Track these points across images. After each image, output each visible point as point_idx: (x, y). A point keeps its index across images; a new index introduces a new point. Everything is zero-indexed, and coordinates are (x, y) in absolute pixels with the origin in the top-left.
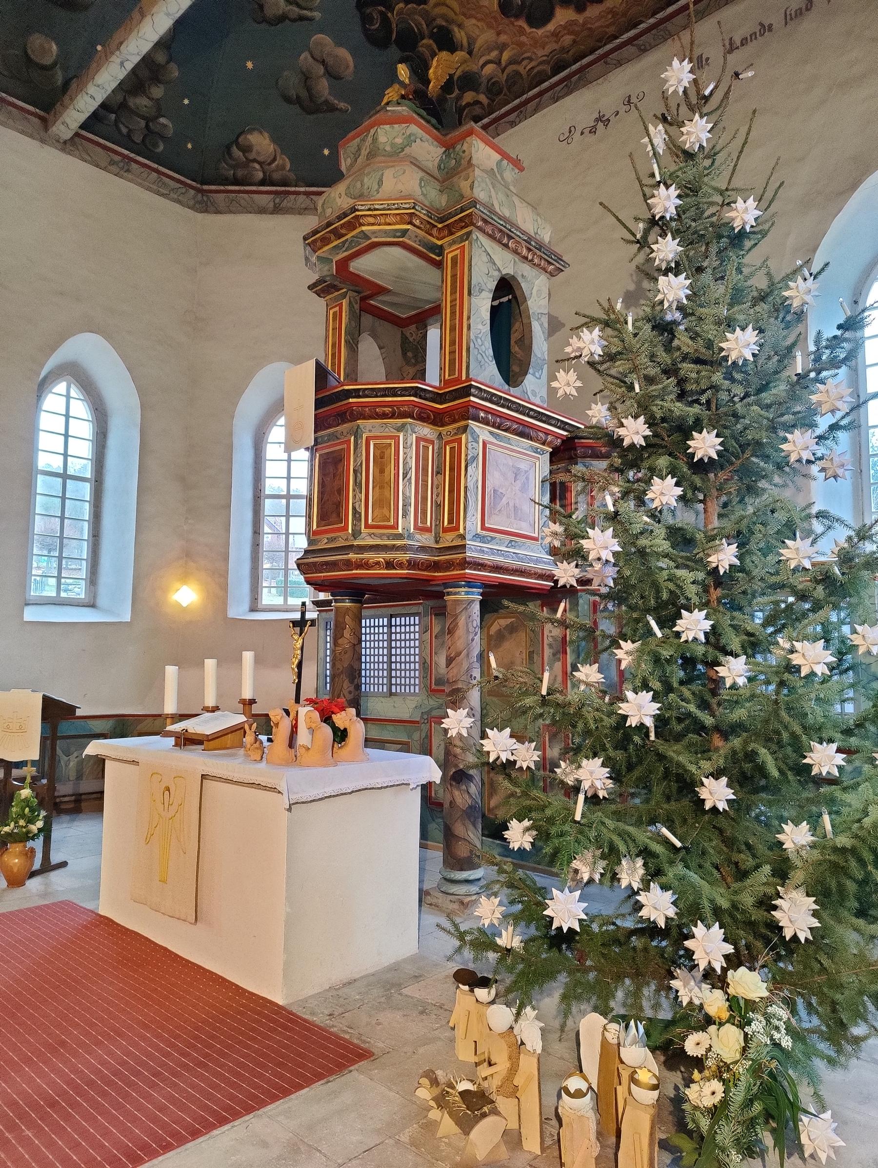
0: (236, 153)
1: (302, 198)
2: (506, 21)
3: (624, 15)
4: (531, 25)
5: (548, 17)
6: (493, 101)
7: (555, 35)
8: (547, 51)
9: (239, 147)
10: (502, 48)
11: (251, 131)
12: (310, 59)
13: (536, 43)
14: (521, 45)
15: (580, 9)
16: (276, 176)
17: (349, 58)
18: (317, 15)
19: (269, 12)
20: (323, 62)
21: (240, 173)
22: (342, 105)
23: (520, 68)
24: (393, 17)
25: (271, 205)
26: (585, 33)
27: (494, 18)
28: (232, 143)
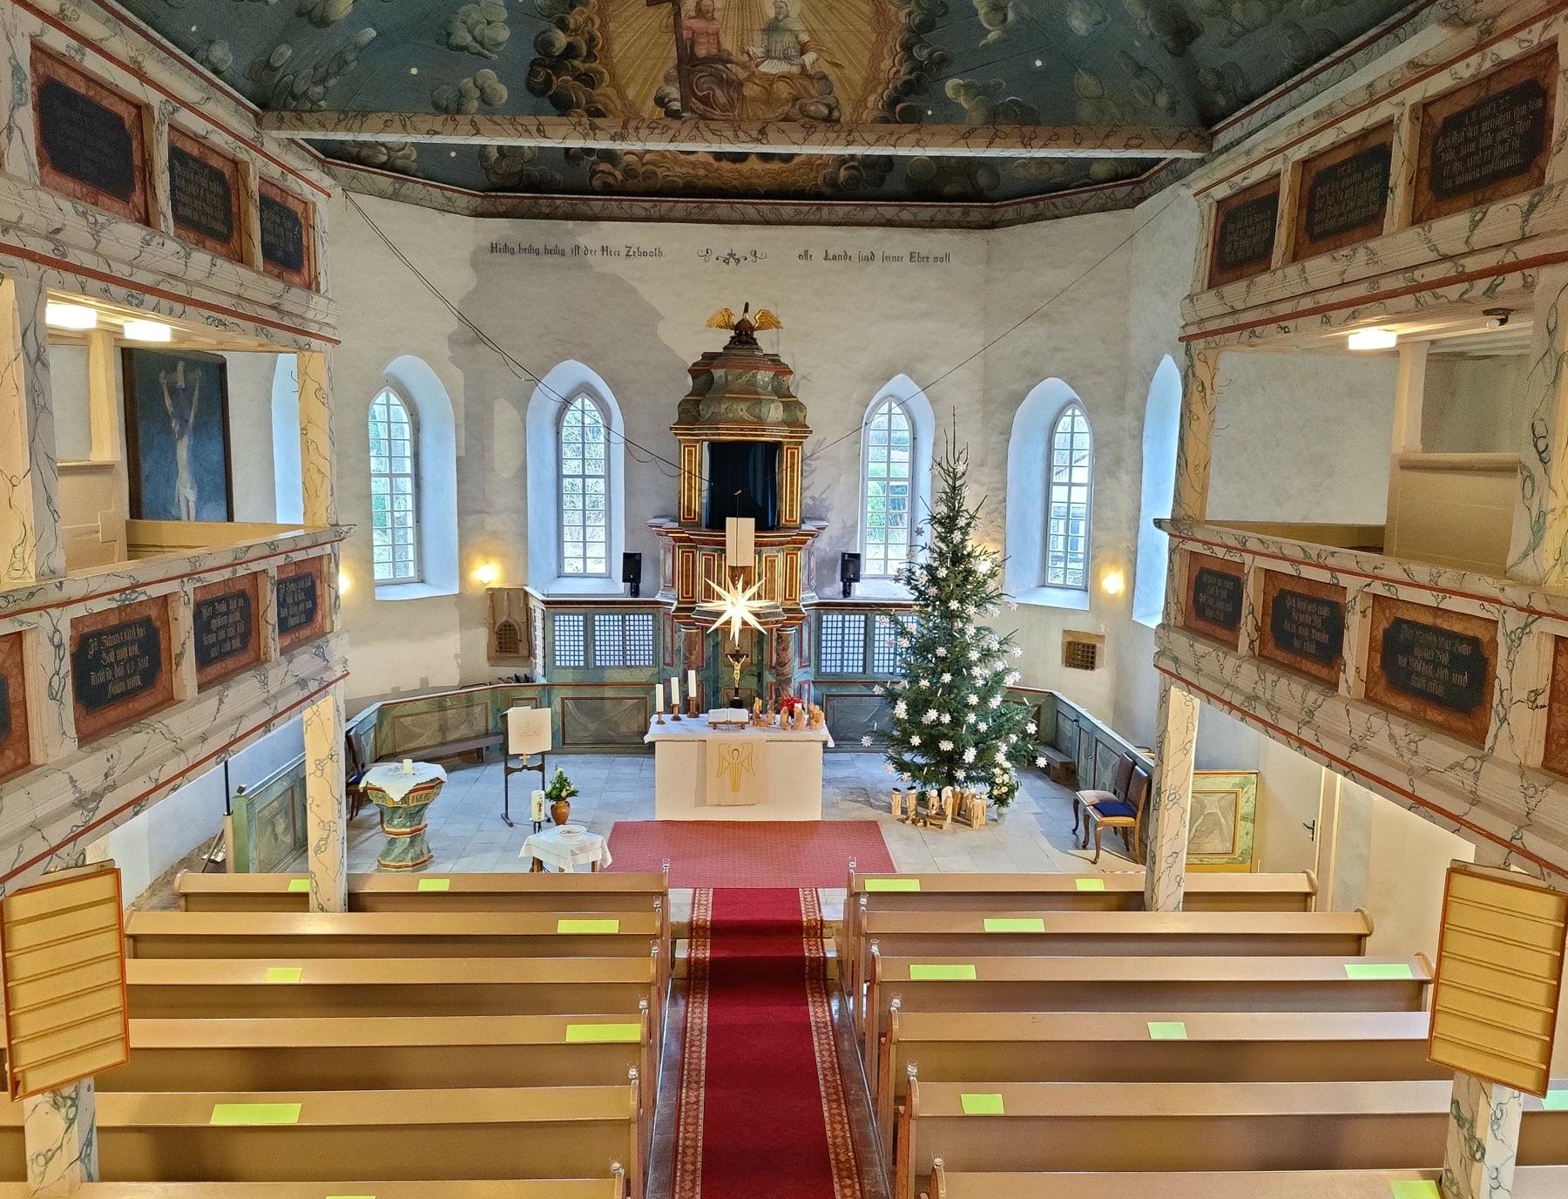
8: (684, 170)
12: (471, 84)
16: (400, 163)
17: (505, 94)
18: (495, 57)
19: (453, 40)
20: (481, 90)
23: (659, 171)
24: (556, 82)
25: (390, 190)
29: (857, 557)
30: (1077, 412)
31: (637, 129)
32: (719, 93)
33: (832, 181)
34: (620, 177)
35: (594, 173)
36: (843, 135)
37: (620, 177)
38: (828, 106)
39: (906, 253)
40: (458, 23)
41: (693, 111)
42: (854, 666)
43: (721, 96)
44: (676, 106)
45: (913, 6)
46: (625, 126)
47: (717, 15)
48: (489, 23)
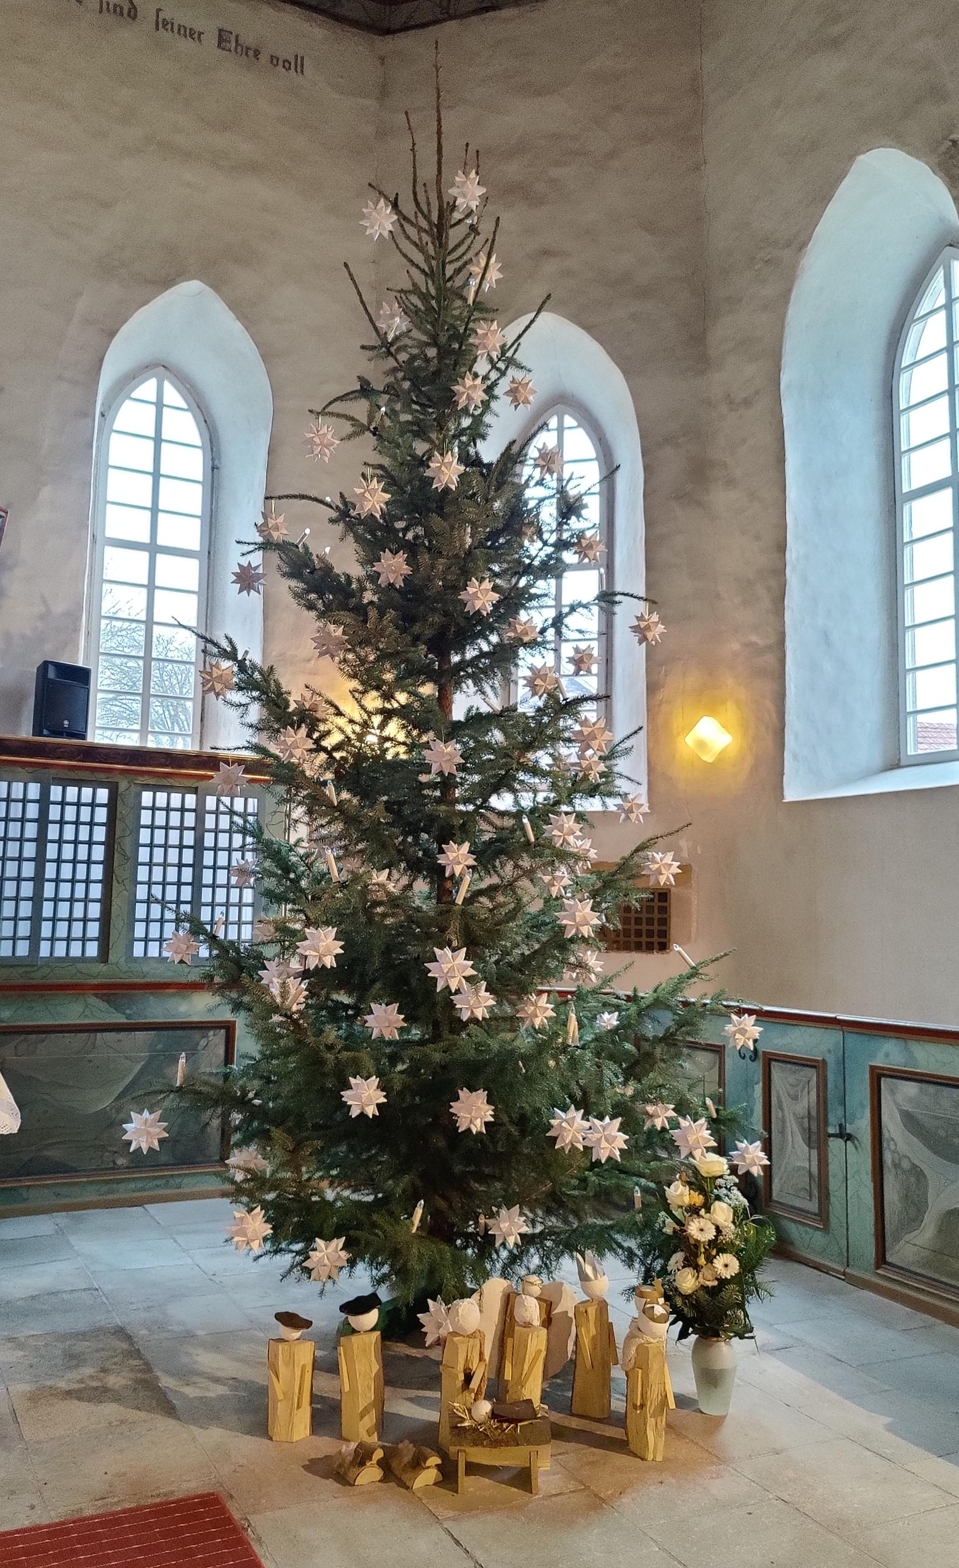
29: (81, 676)
30: (569, 421)
39: (209, 27)
42: (72, 939)
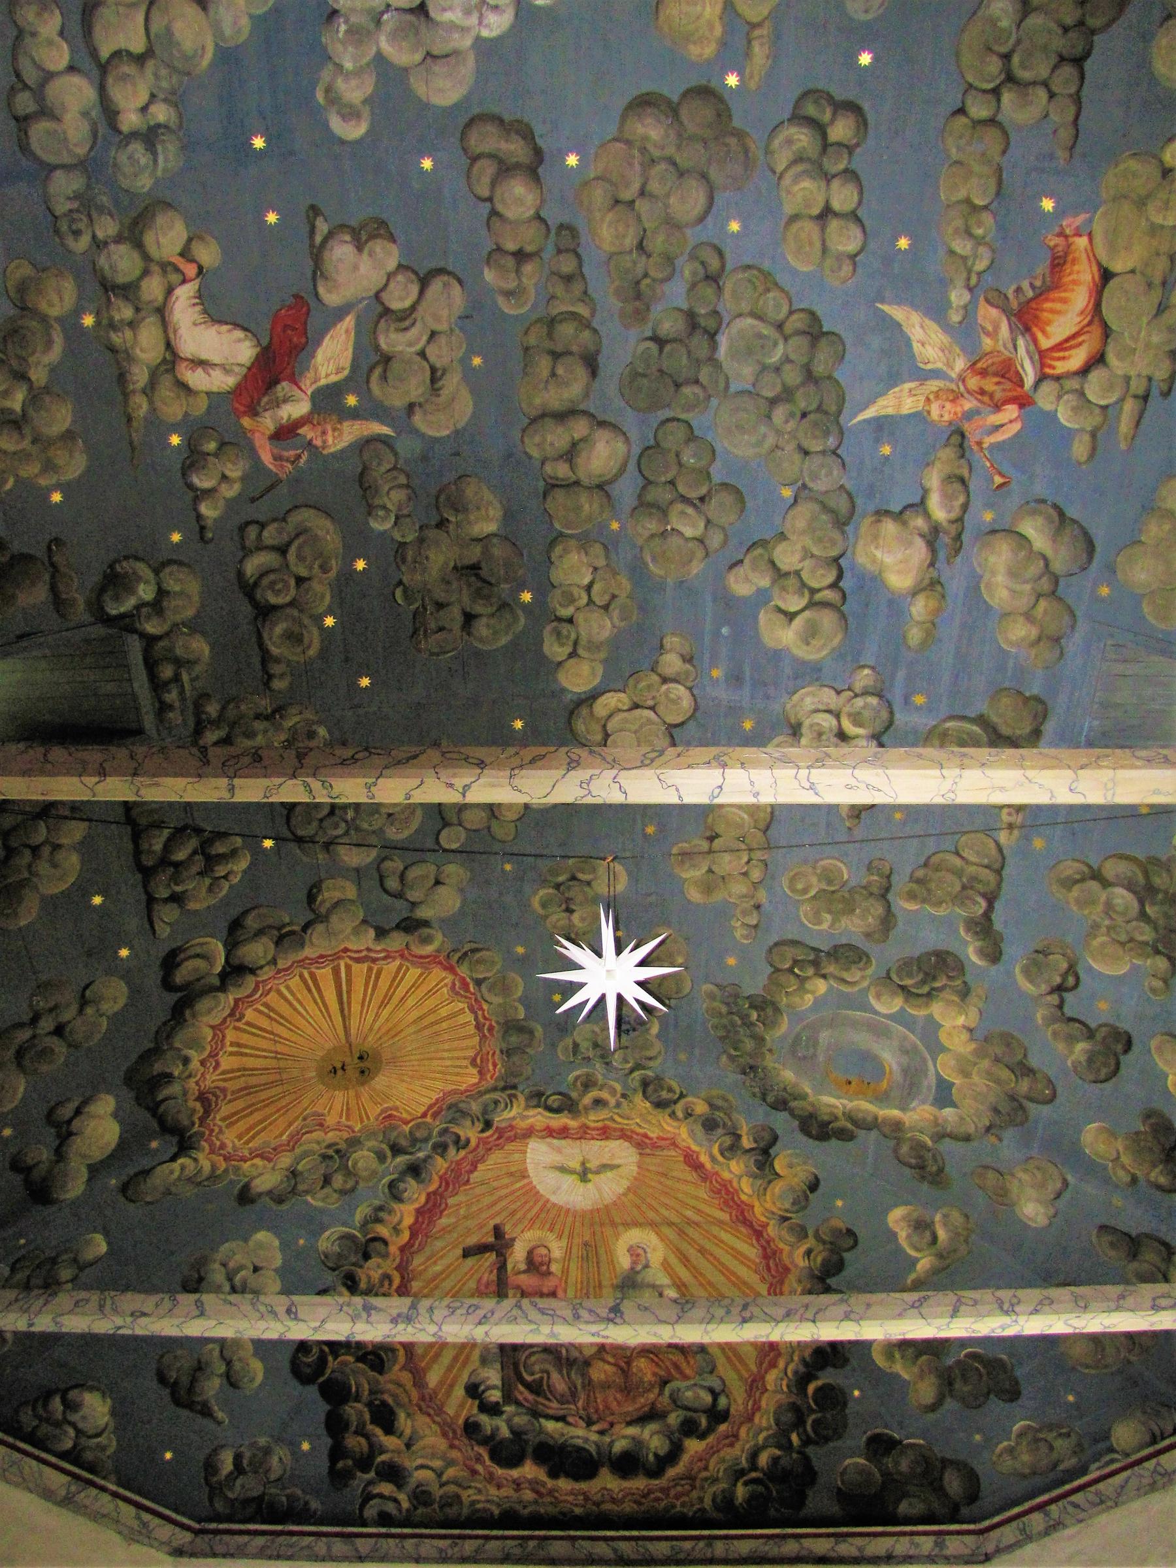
0: (57, 1404)
1: (106, 1498)
2: (466, 1441)
3: (597, 1504)
4: (492, 1458)
5: (514, 1461)
6: (416, 1508)
7: (517, 1485)
8: (504, 1492)
9: (64, 1401)
10: (450, 1463)
11: (92, 1389)
12: (216, 1353)
13: (491, 1478)
14: (474, 1472)
15: (553, 1475)
17: (260, 1377)
20: (229, 1363)
21: (45, 1429)
22: (220, 1415)
26: (549, 1499)
27: (454, 1432)
28: (57, 1391)
31: (431, 1309)
32: (555, 1376)
33: (726, 1502)
34: (405, 1505)
35: (367, 1498)
36: (735, 1311)
37: (405, 1505)
38: (712, 1391)
40: (217, 1266)
41: (518, 1403)
43: (559, 1383)
44: (495, 1396)
45: (810, 1242)
46: (413, 1306)
47: (554, 1268)
48: (256, 1269)
